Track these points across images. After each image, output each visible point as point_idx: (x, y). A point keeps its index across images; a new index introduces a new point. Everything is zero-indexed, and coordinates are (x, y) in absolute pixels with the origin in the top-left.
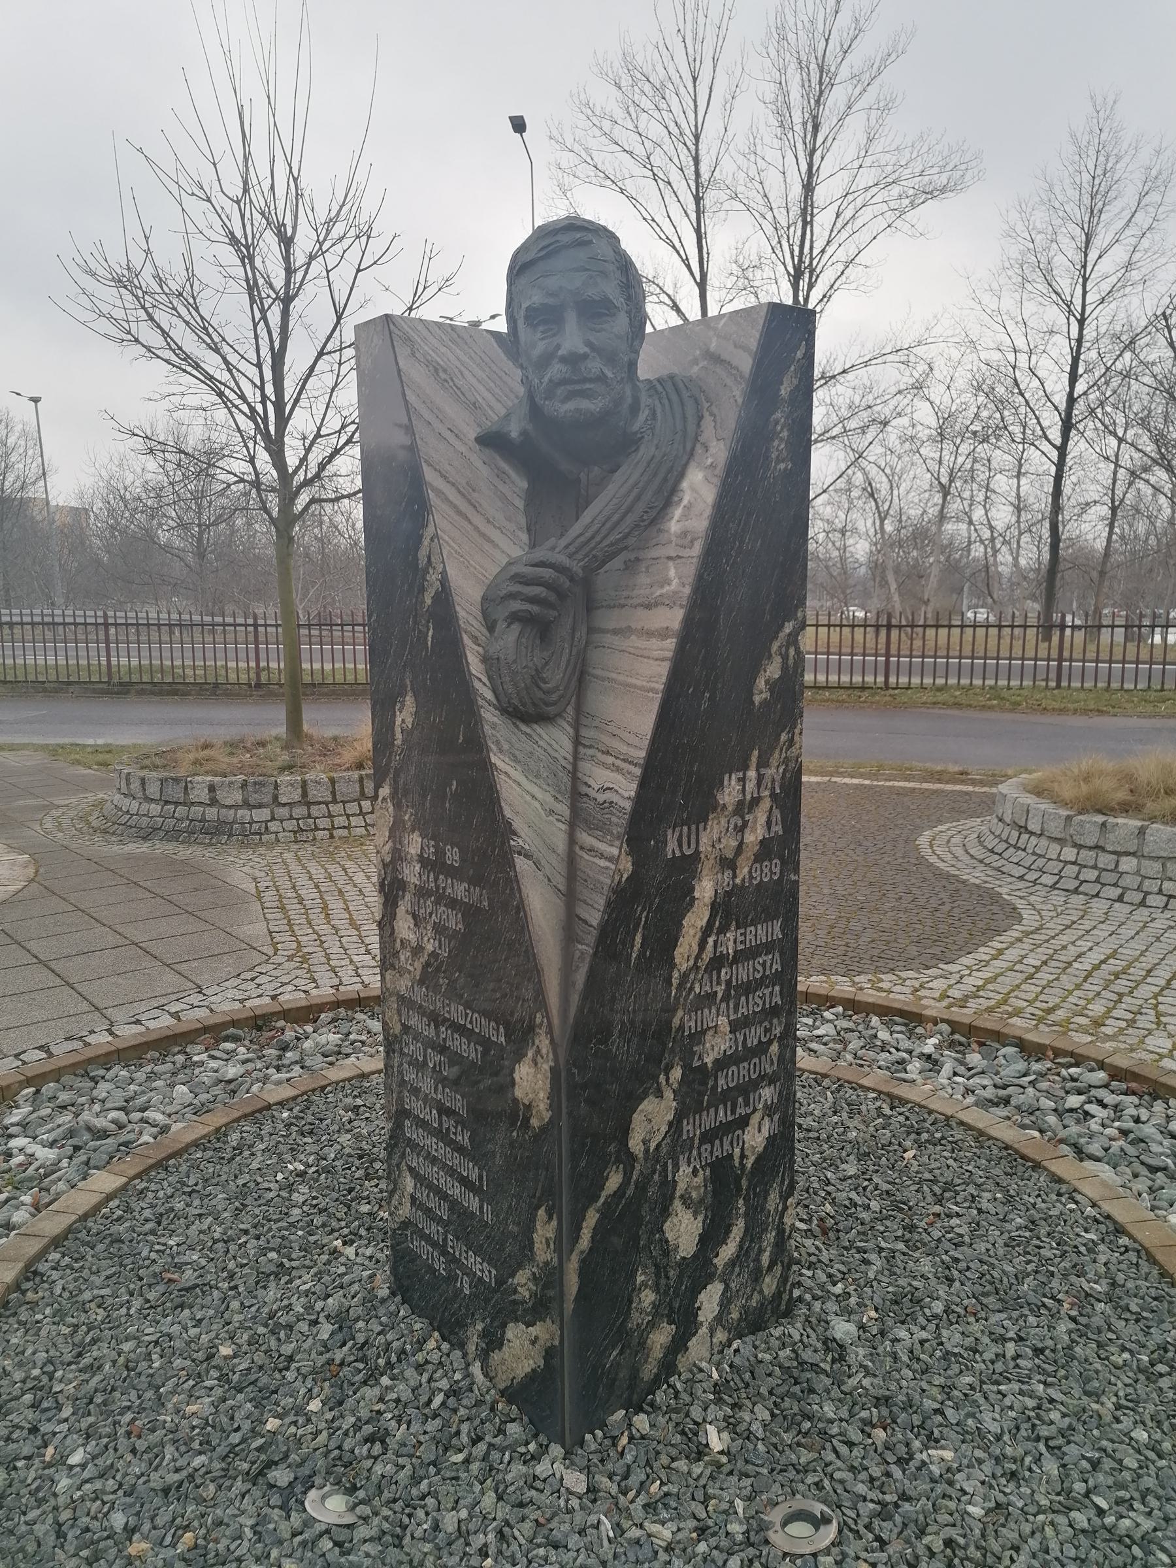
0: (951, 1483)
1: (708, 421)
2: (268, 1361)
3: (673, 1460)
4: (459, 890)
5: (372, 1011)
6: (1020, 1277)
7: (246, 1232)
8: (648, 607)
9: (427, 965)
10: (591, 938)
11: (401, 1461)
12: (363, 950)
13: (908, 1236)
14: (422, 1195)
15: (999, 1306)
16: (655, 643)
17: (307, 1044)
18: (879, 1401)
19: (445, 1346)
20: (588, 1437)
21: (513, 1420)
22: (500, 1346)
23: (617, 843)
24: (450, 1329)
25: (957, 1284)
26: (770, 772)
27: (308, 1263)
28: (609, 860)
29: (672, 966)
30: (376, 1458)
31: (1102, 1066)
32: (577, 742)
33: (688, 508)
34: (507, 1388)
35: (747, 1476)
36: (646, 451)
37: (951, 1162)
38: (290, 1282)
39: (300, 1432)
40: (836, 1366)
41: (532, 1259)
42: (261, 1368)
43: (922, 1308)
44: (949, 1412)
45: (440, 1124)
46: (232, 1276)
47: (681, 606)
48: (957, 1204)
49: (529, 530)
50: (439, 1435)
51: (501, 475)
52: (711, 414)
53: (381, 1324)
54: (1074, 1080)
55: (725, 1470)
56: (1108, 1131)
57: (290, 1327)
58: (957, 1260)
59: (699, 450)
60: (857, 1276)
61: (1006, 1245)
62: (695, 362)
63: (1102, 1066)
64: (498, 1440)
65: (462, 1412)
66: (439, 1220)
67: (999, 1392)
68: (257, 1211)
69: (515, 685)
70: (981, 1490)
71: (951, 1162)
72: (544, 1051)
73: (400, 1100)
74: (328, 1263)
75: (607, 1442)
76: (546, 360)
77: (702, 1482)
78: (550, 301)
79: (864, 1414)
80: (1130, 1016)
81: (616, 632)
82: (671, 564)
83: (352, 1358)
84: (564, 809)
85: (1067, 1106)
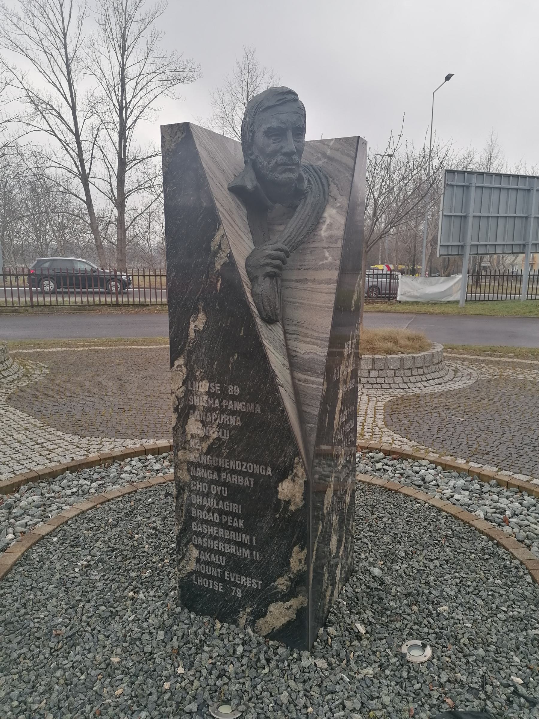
0: (452, 618)
1: (333, 187)
2: (140, 658)
3: (351, 642)
4: (239, 406)
5: (48, 480)
6: (421, 535)
7: (80, 601)
8: (316, 270)
9: (212, 444)
10: (316, 420)
11: (241, 681)
12: (14, 451)
13: (372, 529)
14: (206, 556)
15: (422, 548)
16: (324, 286)
17: (23, 504)
18: (408, 595)
19: (226, 625)
20: (315, 644)
21: (278, 647)
22: (264, 616)
23: (322, 377)
24: (227, 615)
25: (402, 543)
26: (354, 341)
27: (123, 607)
28: (315, 384)
29: (333, 429)
30: (227, 684)
31: (380, 450)
32: (285, 332)
33: (330, 225)
34: (269, 634)
35: (382, 639)
36: (310, 199)
37: (366, 497)
38: (121, 618)
39: (183, 684)
40: (383, 586)
41: (289, 570)
42: (139, 662)
43: (396, 556)
44: (434, 592)
45: (221, 519)
46: (88, 624)
47: (336, 269)
48: (380, 512)
49: (252, 233)
50: (249, 664)
51: (238, 206)
52: (335, 184)
53: (185, 624)
54: (373, 458)
55: (372, 638)
56: (396, 475)
57: (140, 639)
58: (396, 534)
59: (331, 200)
60: (365, 549)
61: (408, 525)
62: (319, 159)
63: (380, 450)
64: (277, 657)
65: (254, 651)
66: (219, 566)
67: (444, 580)
68: (77, 589)
69: (270, 307)
70: (464, 617)
71: (366, 497)
72: (300, 474)
73: (189, 512)
74: (133, 604)
75: (323, 643)
76: (274, 153)
77: (369, 647)
78: (282, 126)
79: (405, 602)
80: (371, 431)
81: (297, 281)
82: (325, 250)
83: (182, 644)
84: (287, 363)
85: (377, 468)
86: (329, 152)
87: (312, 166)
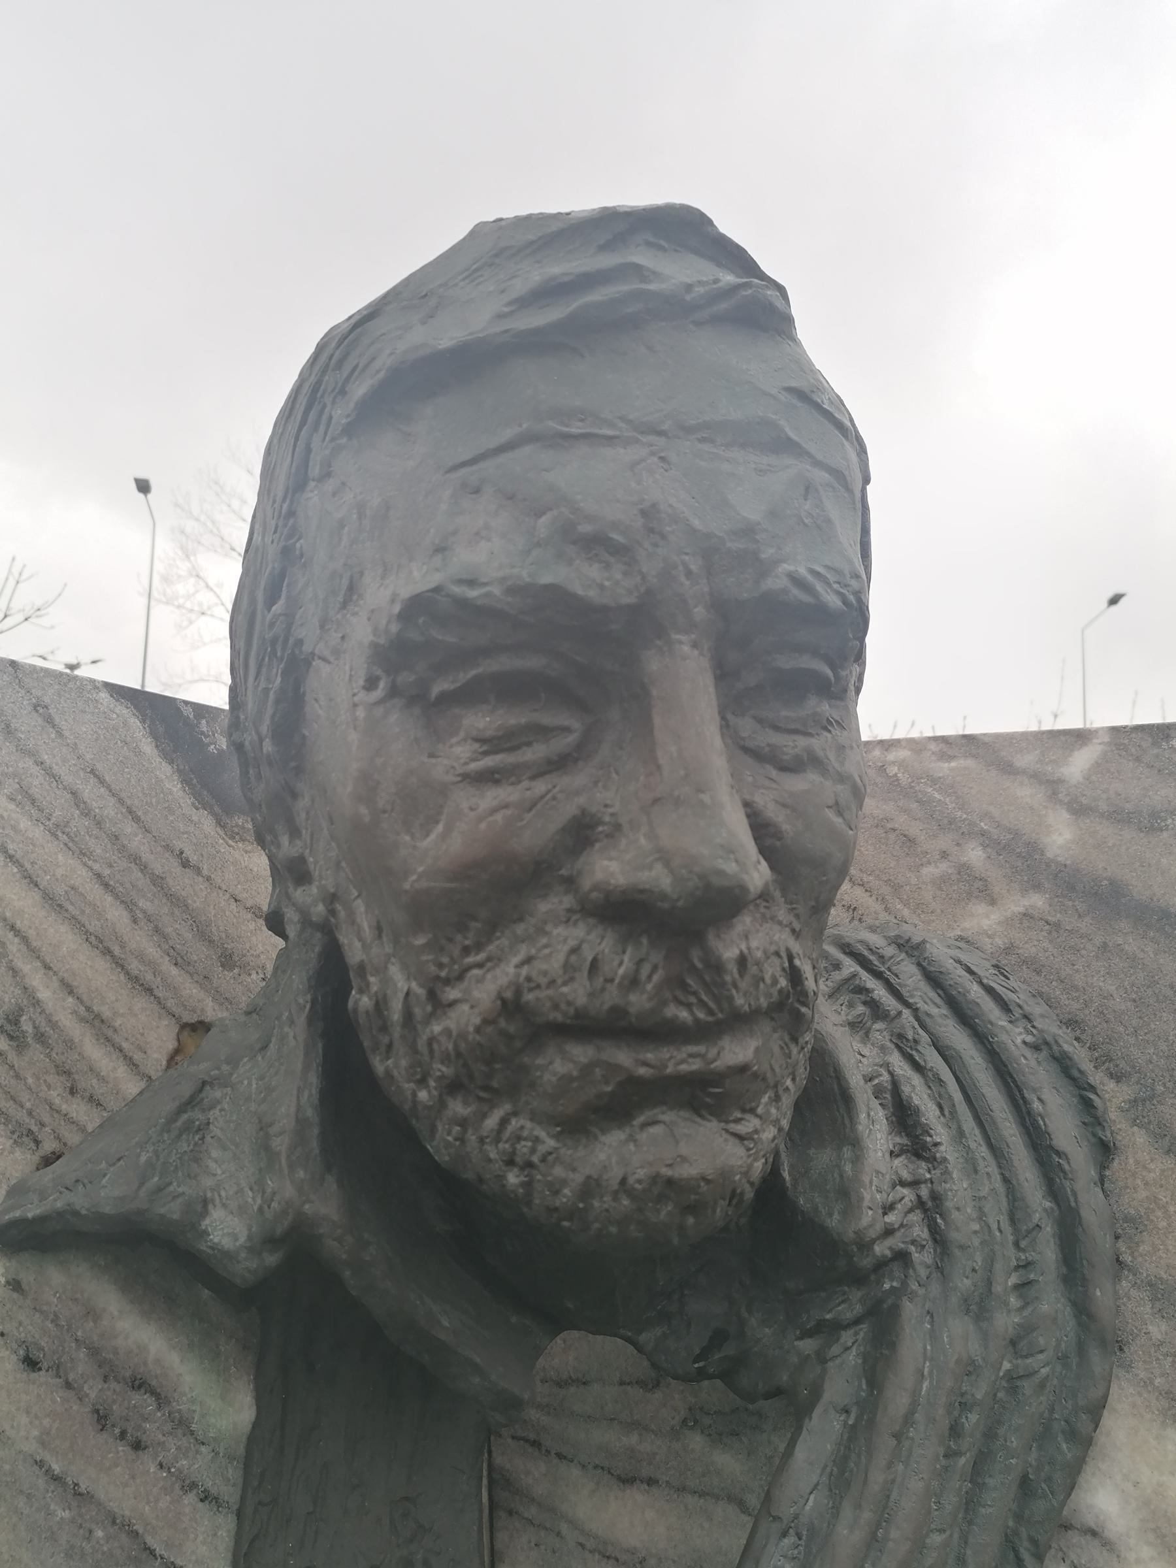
36: (936, 1342)
62: (978, 888)
76: (492, 896)
78: (586, 579)
86: (1060, 836)
87: (911, 948)
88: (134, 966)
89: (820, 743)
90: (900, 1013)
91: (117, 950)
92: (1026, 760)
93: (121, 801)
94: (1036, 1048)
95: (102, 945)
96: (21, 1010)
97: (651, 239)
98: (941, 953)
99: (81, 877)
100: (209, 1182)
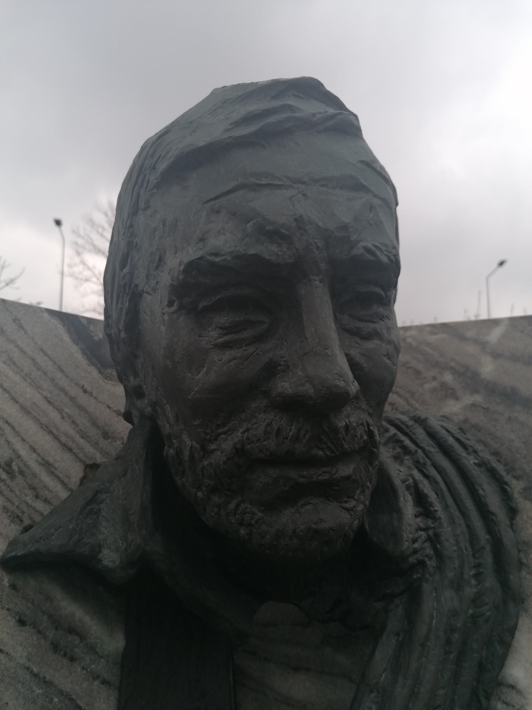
36: (439, 602)
62: (449, 393)
76: (229, 400)
78: (270, 251)
86: (488, 368)
87: (421, 421)
88: (63, 439)
89: (379, 326)
90: (416, 452)
91: (55, 432)
92: (470, 334)
93: (55, 363)
94: (479, 465)
95: (48, 429)
96: (11, 460)
97: (296, 93)
98: (434, 423)
99: (38, 398)
100: (101, 537)
